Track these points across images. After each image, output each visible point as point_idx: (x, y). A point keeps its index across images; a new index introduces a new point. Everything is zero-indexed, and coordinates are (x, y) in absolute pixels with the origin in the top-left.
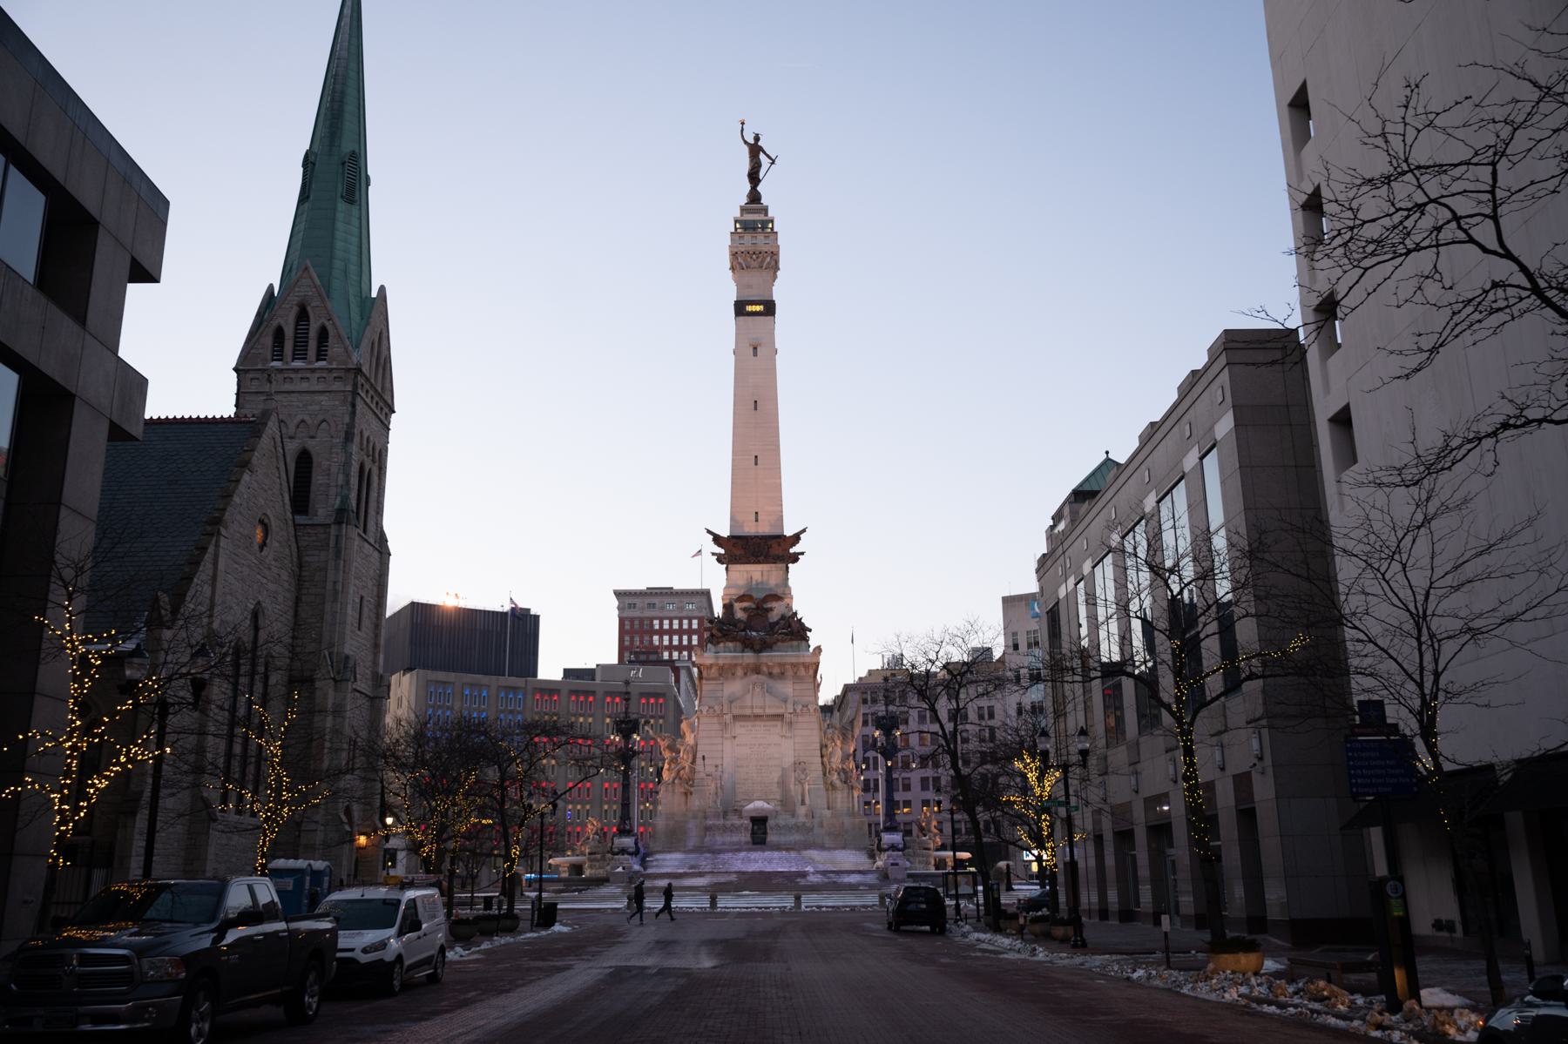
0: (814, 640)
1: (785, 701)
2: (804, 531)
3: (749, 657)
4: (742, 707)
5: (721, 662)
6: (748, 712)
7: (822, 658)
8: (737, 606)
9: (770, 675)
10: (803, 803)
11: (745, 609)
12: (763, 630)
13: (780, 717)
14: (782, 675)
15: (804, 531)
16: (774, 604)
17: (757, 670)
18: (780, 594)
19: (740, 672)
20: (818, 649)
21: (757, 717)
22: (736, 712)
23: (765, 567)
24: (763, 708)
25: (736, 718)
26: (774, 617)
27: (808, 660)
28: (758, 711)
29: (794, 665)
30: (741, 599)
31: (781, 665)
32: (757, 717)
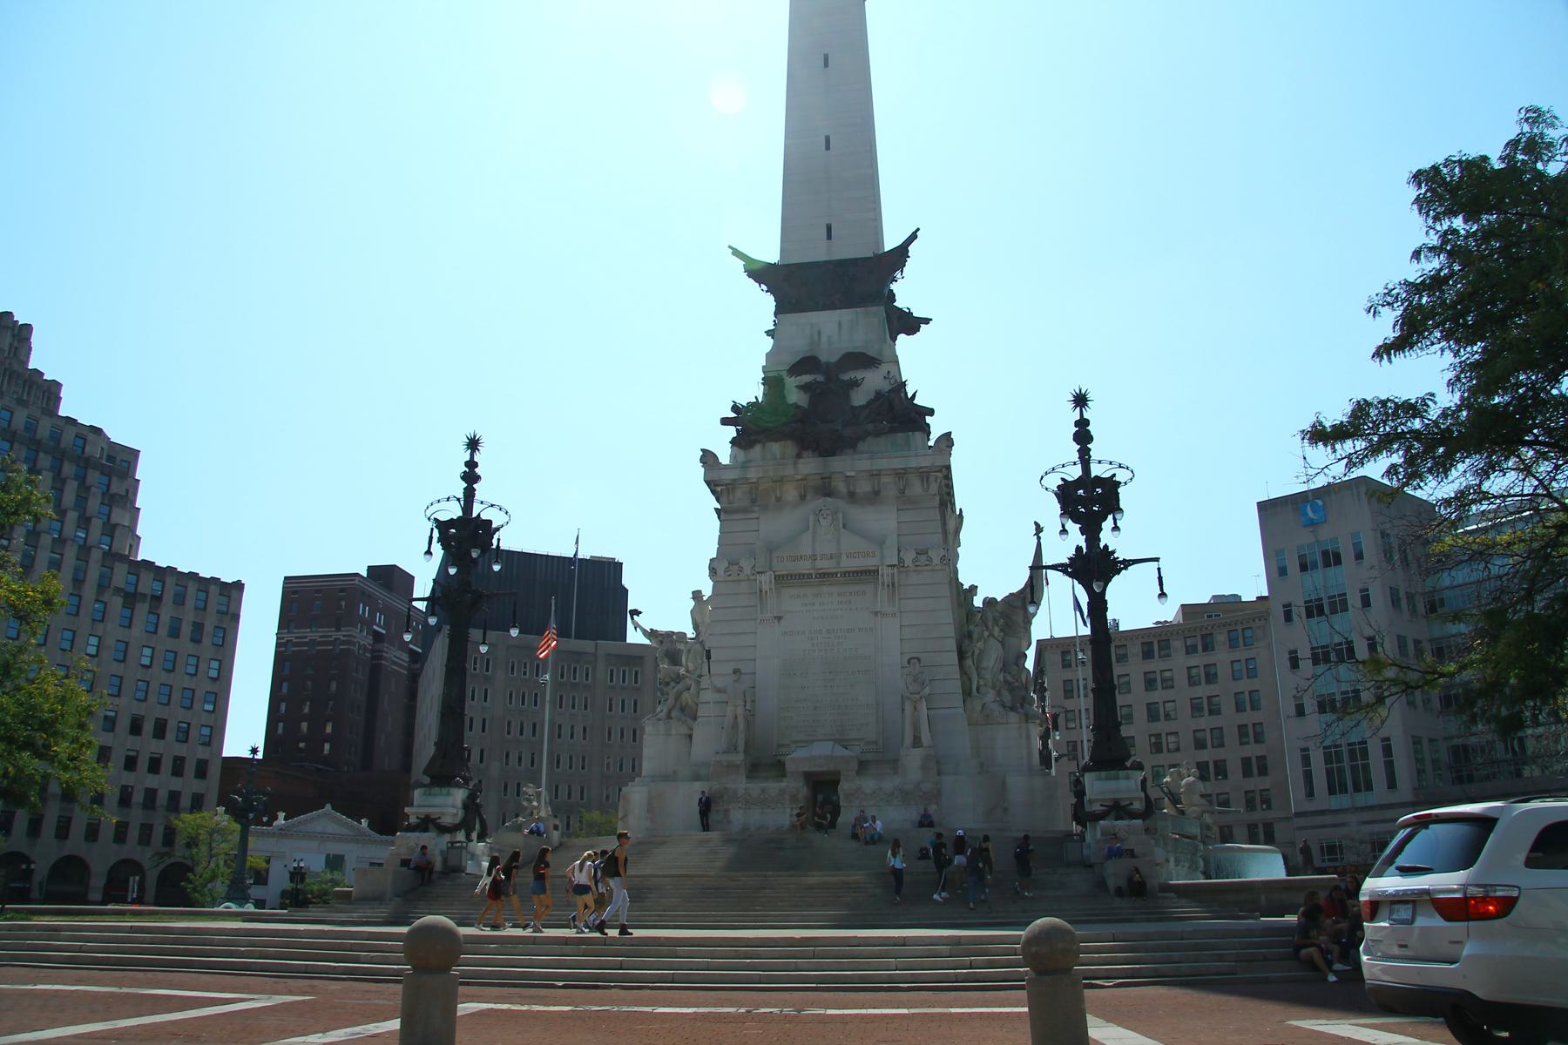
0: (937, 426)
1: (881, 544)
2: (913, 237)
3: (810, 465)
4: (794, 559)
5: (753, 475)
6: (805, 567)
7: (958, 461)
8: (791, 382)
9: (852, 496)
10: (917, 742)
11: (803, 387)
12: (833, 416)
13: (868, 575)
14: (875, 497)
15: (913, 237)
16: (859, 375)
17: (826, 491)
18: (879, 359)
19: (791, 493)
20: (947, 439)
21: (824, 577)
22: (784, 568)
23: (845, 315)
24: (839, 556)
25: (781, 580)
26: (859, 398)
27: (925, 462)
28: (825, 565)
29: (901, 474)
30: (798, 368)
31: (875, 475)
32: (824, 577)
